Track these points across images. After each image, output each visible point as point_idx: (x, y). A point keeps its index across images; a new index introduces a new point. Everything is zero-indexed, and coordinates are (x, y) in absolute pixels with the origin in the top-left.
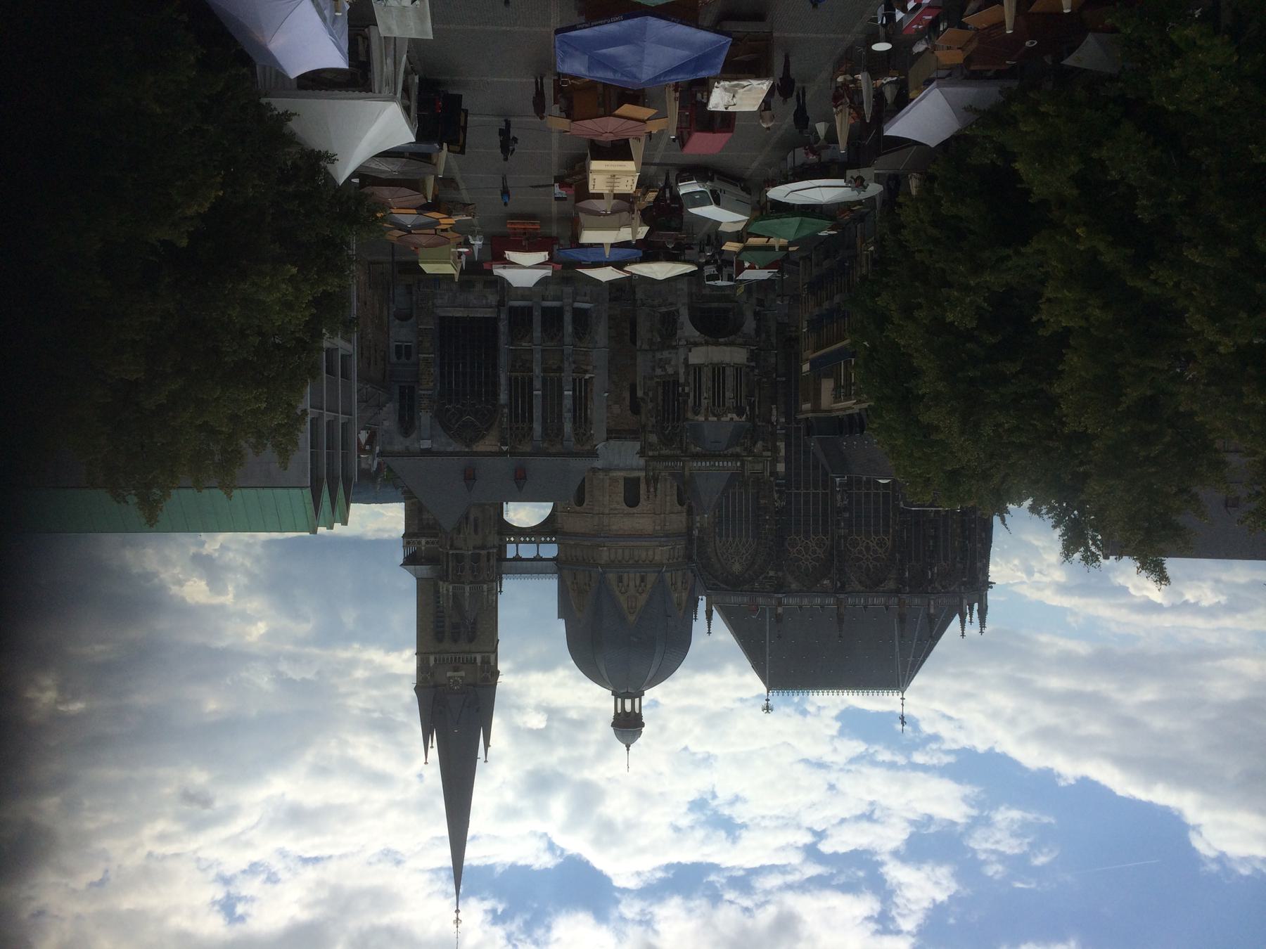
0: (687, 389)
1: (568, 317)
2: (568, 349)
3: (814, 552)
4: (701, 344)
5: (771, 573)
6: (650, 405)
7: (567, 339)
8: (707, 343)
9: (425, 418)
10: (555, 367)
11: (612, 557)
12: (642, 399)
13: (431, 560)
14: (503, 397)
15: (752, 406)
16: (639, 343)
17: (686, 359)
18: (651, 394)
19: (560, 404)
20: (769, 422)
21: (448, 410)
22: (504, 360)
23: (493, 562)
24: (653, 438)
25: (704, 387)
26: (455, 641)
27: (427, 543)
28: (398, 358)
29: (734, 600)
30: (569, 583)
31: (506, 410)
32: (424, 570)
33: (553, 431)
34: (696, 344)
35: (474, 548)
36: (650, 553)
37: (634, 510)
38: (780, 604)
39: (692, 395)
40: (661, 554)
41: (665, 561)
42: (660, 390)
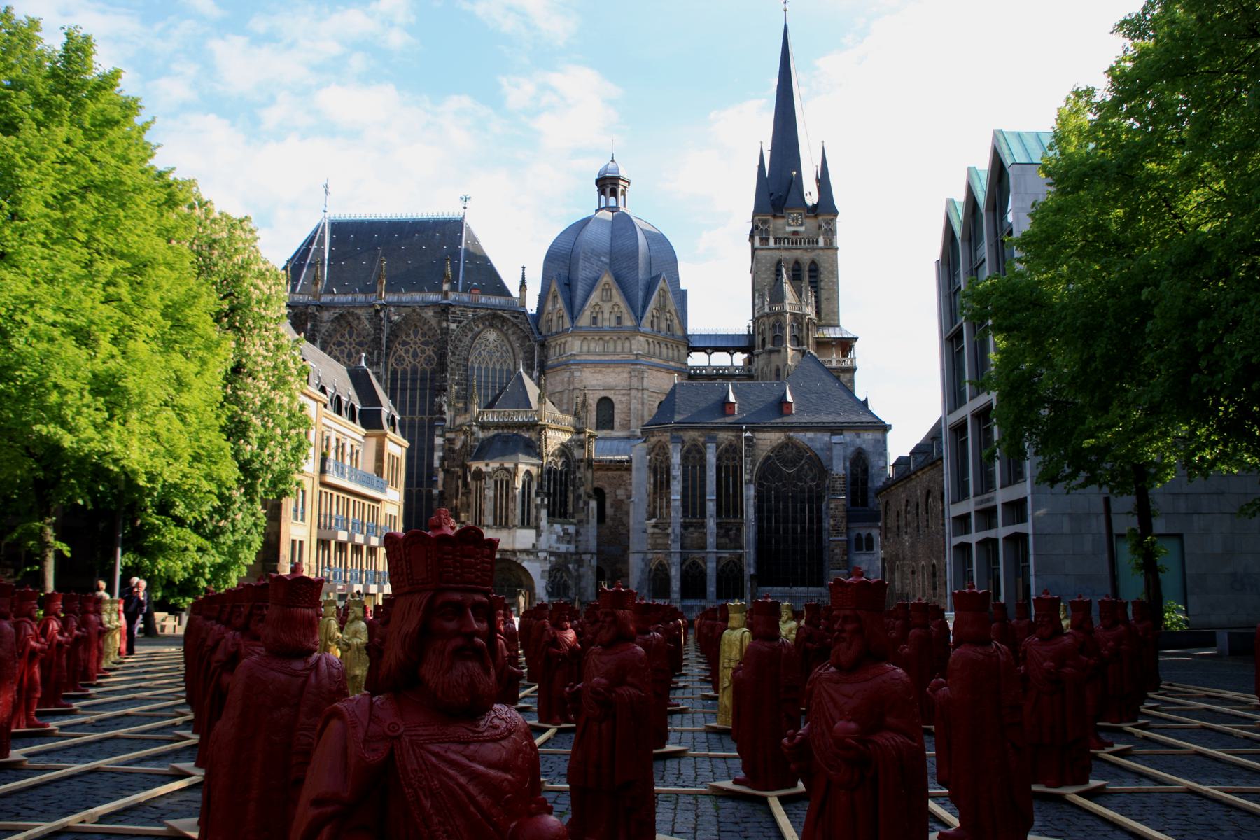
0: (539, 500)
1: (676, 585)
2: (676, 547)
3: (407, 352)
4: (522, 551)
7: (676, 559)
8: (514, 552)
9: (839, 468)
10: (691, 529)
11: (627, 344)
12: (590, 497)
13: (823, 344)
14: (750, 492)
15: (466, 484)
16: (594, 562)
17: (538, 535)
18: (581, 504)
19: (685, 489)
20: (446, 472)
21: (813, 480)
22: (749, 534)
23: (758, 340)
25: (519, 500)
26: (797, 263)
28: (869, 535)
29: (495, 300)
30: (676, 321)
31: (746, 477)
32: (831, 333)
33: (693, 458)
34: (527, 552)
36: (585, 348)
37: (603, 394)
40: (575, 346)
41: (570, 339)
42: (570, 509)
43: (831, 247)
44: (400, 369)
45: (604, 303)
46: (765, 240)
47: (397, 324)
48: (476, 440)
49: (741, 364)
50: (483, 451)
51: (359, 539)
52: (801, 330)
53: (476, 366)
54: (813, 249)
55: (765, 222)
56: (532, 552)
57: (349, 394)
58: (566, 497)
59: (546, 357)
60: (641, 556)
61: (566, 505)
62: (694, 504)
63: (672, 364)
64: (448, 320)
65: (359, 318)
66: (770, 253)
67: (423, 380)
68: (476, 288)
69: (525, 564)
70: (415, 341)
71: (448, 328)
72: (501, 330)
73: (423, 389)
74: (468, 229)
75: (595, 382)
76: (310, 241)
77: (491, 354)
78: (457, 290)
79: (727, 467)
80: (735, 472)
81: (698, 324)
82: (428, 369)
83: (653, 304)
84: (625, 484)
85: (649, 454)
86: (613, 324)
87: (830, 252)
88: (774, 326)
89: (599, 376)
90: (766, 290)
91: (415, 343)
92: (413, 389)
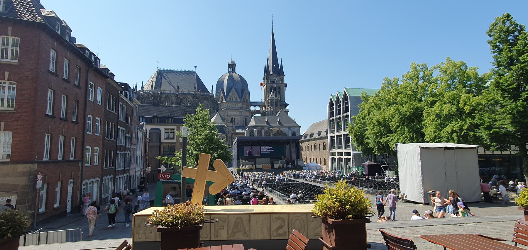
38: (195, 92)
46: (268, 81)
81: (252, 100)
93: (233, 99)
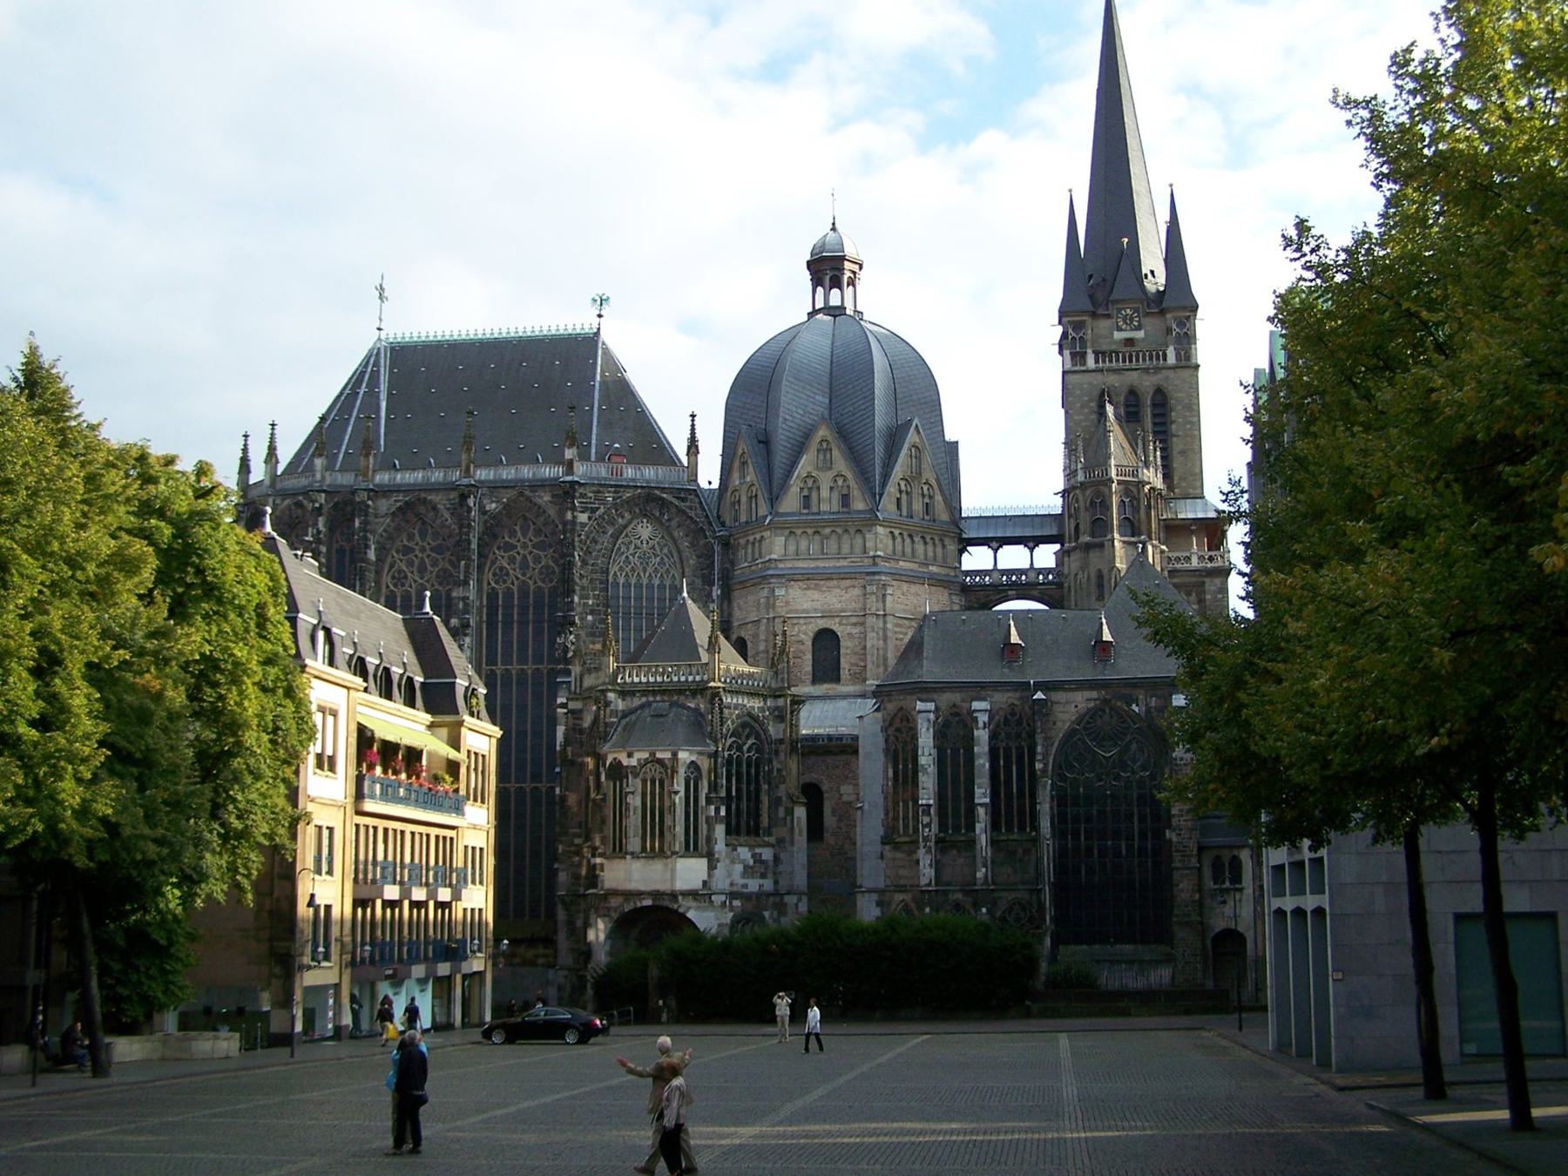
3: (512, 560)
5: (583, 518)
6: (782, 791)
8: (673, 895)
11: (858, 540)
13: (1176, 531)
17: (712, 867)
21: (1144, 769)
24: (774, 730)
26: (1133, 393)
27: (1188, 559)
29: (649, 473)
31: (1038, 766)
34: (693, 894)
35: (1101, 546)
36: (792, 548)
37: (822, 624)
39: (702, 802)
40: (776, 546)
43: (1188, 365)
44: (500, 589)
45: (820, 474)
46: (1078, 357)
47: (495, 516)
48: (614, 713)
49: (1051, 563)
50: (630, 727)
51: (419, 894)
52: (1136, 509)
53: (622, 581)
54: (1158, 369)
55: (1078, 326)
56: (701, 895)
57: (404, 662)
58: (758, 801)
59: (733, 563)
60: (875, 897)
61: (758, 816)
62: (956, 809)
63: (933, 569)
64: (574, 509)
65: (434, 508)
66: (1086, 378)
67: (539, 605)
68: (618, 453)
69: (690, 915)
70: (523, 541)
71: (574, 522)
72: (659, 520)
73: (538, 622)
74: (606, 352)
75: (805, 606)
76: (368, 358)
77: (644, 560)
78: (588, 459)
79: (1007, 750)
80: (1020, 758)
82: (546, 587)
83: (898, 471)
84: (851, 776)
85: (884, 729)
86: (835, 509)
87: (1185, 373)
88: (1092, 502)
89: (816, 595)
90: (1084, 444)
91: (525, 546)
92: (523, 624)
93: (827, 501)
